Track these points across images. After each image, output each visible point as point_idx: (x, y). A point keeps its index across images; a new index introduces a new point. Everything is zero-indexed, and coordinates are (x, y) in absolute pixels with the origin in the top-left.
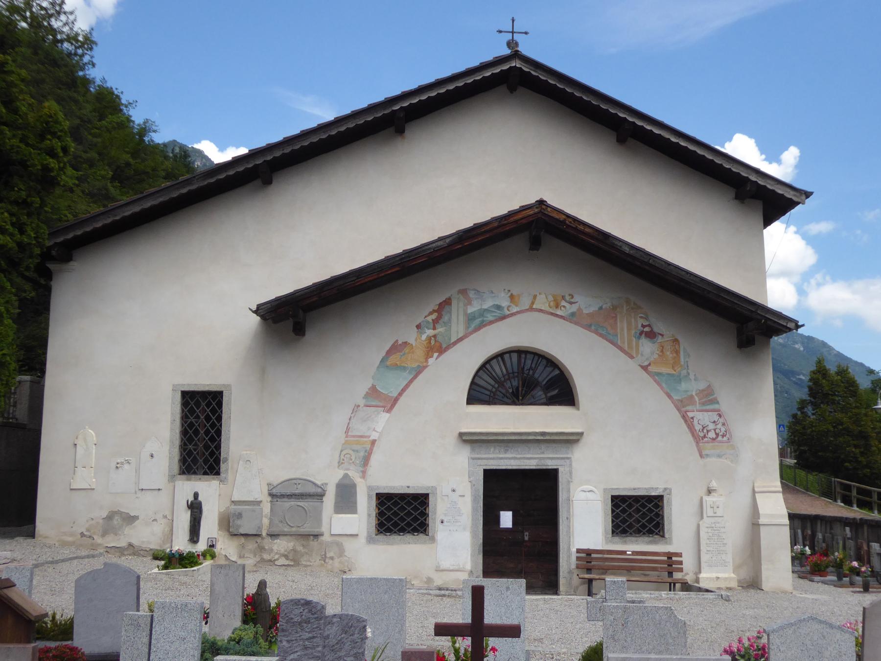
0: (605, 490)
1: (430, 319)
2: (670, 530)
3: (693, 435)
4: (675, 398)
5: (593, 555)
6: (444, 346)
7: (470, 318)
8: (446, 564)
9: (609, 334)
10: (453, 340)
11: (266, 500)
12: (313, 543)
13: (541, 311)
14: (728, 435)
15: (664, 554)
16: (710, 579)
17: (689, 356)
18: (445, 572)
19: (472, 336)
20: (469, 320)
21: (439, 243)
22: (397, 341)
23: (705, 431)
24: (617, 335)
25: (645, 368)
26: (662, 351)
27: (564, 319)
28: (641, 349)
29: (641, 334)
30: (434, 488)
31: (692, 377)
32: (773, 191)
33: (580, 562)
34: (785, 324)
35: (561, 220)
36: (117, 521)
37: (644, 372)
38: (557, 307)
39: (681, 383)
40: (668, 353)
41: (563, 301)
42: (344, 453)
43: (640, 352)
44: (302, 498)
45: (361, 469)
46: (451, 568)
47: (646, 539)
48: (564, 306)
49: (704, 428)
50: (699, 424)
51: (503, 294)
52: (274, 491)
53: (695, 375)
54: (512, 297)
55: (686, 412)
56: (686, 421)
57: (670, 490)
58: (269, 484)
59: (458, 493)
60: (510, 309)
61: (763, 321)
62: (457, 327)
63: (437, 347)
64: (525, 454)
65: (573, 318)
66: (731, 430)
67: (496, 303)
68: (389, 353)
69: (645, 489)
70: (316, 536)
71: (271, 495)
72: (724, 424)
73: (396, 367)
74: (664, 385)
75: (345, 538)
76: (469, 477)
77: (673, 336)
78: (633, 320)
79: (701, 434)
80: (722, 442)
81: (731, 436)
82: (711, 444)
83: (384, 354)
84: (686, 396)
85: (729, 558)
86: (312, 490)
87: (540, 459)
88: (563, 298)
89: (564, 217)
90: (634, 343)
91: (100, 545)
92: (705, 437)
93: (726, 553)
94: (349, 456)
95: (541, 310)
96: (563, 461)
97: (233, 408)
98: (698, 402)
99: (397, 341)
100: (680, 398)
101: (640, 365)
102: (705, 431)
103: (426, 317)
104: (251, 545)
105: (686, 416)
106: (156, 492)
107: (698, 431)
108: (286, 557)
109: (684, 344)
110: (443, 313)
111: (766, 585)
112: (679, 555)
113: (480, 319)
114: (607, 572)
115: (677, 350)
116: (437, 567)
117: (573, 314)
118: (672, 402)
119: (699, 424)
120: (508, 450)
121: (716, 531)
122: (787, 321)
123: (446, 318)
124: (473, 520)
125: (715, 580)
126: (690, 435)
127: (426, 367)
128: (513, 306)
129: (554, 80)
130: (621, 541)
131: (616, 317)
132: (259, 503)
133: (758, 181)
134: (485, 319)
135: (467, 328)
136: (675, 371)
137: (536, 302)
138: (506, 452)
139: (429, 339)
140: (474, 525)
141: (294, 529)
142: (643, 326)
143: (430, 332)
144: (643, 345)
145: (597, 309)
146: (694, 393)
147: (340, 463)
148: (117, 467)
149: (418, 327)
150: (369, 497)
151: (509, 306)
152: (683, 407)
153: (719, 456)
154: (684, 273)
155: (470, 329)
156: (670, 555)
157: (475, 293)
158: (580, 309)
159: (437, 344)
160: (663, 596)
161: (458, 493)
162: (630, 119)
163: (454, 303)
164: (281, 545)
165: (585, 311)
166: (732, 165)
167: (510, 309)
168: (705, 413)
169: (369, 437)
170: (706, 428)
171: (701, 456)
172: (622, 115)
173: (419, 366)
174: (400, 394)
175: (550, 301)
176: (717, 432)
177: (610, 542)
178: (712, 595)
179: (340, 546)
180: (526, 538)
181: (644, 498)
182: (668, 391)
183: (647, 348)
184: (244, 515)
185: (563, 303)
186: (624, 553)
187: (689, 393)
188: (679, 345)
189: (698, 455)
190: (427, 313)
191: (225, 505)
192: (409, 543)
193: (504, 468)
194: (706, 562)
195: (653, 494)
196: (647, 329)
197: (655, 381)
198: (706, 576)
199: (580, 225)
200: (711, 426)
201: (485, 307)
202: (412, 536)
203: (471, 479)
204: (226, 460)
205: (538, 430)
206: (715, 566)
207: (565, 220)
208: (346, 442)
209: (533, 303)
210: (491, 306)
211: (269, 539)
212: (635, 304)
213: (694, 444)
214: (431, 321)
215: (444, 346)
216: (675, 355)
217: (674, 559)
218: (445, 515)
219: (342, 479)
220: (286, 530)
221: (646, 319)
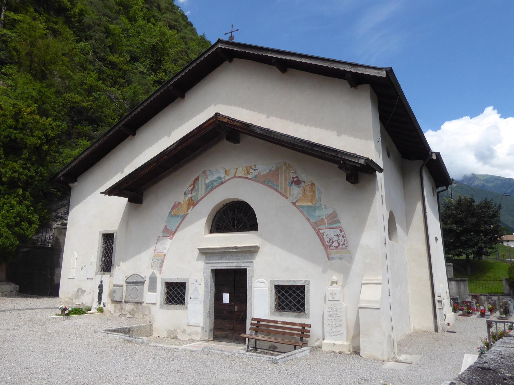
0: (271, 281)
1: (190, 189)
2: (309, 309)
4: (312, 221)
5: (261, 323)
6: (195, 202)
7: (207, 186)
8: (192, 322)
9: (275, 185)
10: (199, 198)
12: (140, 307)
13: (240, 177)
14: (346, 244)
15: (300, 325)
16: (329, 345)
17: (321, 193)
18: (191, 327)
19: (208, 195)
20: (206, 187)
21: (172, 147)
22: (176, 202)
23: (331, 242)
24: (279, 185)
25: (294, 204)
26: (304, 192)
27: (251, 180)
28: (292, 192)
29: (292, 183)
30: (188, 279)
31: (323, 206)
32: (362, 74)
33: (253, 326)
34: (357, 161)
35: (226, 122)
36: (80, 292)
37: (294, 206)
38: (248, 173)
39: (316, 211)
40: (308, 193)
41: (251, 169)
42: (153, 261)
43: (291, 194)
44: (137, 284)
45: (160, 269)
46: (194, 325)
47: (295, 314)
48: (251, 173)
49: (330, 240)
50: (327, 237)
53: (325, 205)
54: (226, 171)
55: (319, 230)
56: (319, 236)
57: (309, 281)
58: (126, 277)
59: (198, 282)
60: (225, 178)
61: (342, 161)
63: (192, 203)
64: (230, 260)
65: (256, 179)
66: (348, 240)
67: (218, 176)
68: (173, 208)
69: (294, 280)
70: (141, 303)
71: (127, 282)
72: (343, 237)
73: (176, 216)
74: (305, 213)
75: (151, 305)
76: (204, 274)
77: (311, 181)
78: (288, 175)
79: (329, 244)
80: (343, 249)
81: (348, 244)
83: (170, 209)
84: (319, 219)
85: (344, 330)
86: (140, 280)
87: (238, 262)
88: (251, 167)
90: (288, 188)
91: (74, 303)
92: (331, 246)
93: (342, 327)
94: (155, 262)
95: (239, 176)
96: (249, 264)
97: (117, 241)
98: (326, 223)
99: (176, 202)
100: (315, 221)
101: (291, 202)
102: (331, 242)
103: (188, 188)
104: (118, 306)
105: (319, 233)
106: (91, 280)
107: (326, 242)
108: (130, 312)
109: (317, 185)
110: (196, 185)
111: (363, 353)
112: (309, 326)
113: (211, 186)
114: (270, 334)
115: (313, 190)
116: (188, 323)
117: (256, 176)
118: (310, 224)
119: (327, 237)
120: (222, 258)
121: (335, 311)
122: (358, 159)
123: (196, 187)
125: (332, 345)
126: (321, 245)
127: (187, 214)
128: (226, 176)
130: (279, 314)
131: (278, 175)
132: (122, 286)
133: (351, 70)
134: (213, 185)
135: (206, 191)
136: (312, 204)
137: (237, 172)
138: (221, 259)
139: (189, 199)
140: (205, 301)
141: (133, 299)
142: (294, 178)
143: (189, 196)
144: (293, 190)
145: (268, 171)
146: (324, 218)
147: (152, 266)
148: (81, 269)
149: (185, 194)
150: (162, 284)
151: (225, 177)
152: (317, 227)
153: (340, 259)
154: (291, 139)
155: (207, 192)
156: (304, 326)
157: (209, 172)
158: (259, 173)
159: (192, 202)
160: (236, 354)
161: (198, 282)
162: (274, 56)
163: (200, 178)
164: (129, 307)
165: (262, 174)
166: (334, 65)
167: (225, 178)
168: (332, 230)
170: (332, 240)
171: (329, 259)
172: (269, 55)
173: (184, 214)
174: (176, 230)
175: (244, 170)
176: (339, 242)
177: (273, 314)
178: (266, 358)
179: (149, 308)
180: (236, 310)
181: (295, 287)
182: (308, 217)
183: (296, 191)
185: (251, 171)
186: (276, 322)
187: (321, 218)
188: (315, 186)
189: (327, 258)
191: (111, 287)
192: (177, 309)
193: (220, 268)
194: (328, 332)
195: (298, 284)
196: (295, 179)
197: (300, 211)
198: (327, 342)
199: (235, 122)
200: (335, 238)
201: (214, 179)
202: (180, 306)
203: (205, 274)
204: (113, 265)
205: (233, 246)
206: (334, 335)
207: (228, 121)
209: (236, 173)
210: (216, 178)
211: (124, 304)
212: (289, 165)
213: (324, 251)
214: (190, 190)
215: (195, 202)
216: (312, 193)
217: (306, 328)
218: (192, 294)
219: (152, 274)
220: (130, 299)
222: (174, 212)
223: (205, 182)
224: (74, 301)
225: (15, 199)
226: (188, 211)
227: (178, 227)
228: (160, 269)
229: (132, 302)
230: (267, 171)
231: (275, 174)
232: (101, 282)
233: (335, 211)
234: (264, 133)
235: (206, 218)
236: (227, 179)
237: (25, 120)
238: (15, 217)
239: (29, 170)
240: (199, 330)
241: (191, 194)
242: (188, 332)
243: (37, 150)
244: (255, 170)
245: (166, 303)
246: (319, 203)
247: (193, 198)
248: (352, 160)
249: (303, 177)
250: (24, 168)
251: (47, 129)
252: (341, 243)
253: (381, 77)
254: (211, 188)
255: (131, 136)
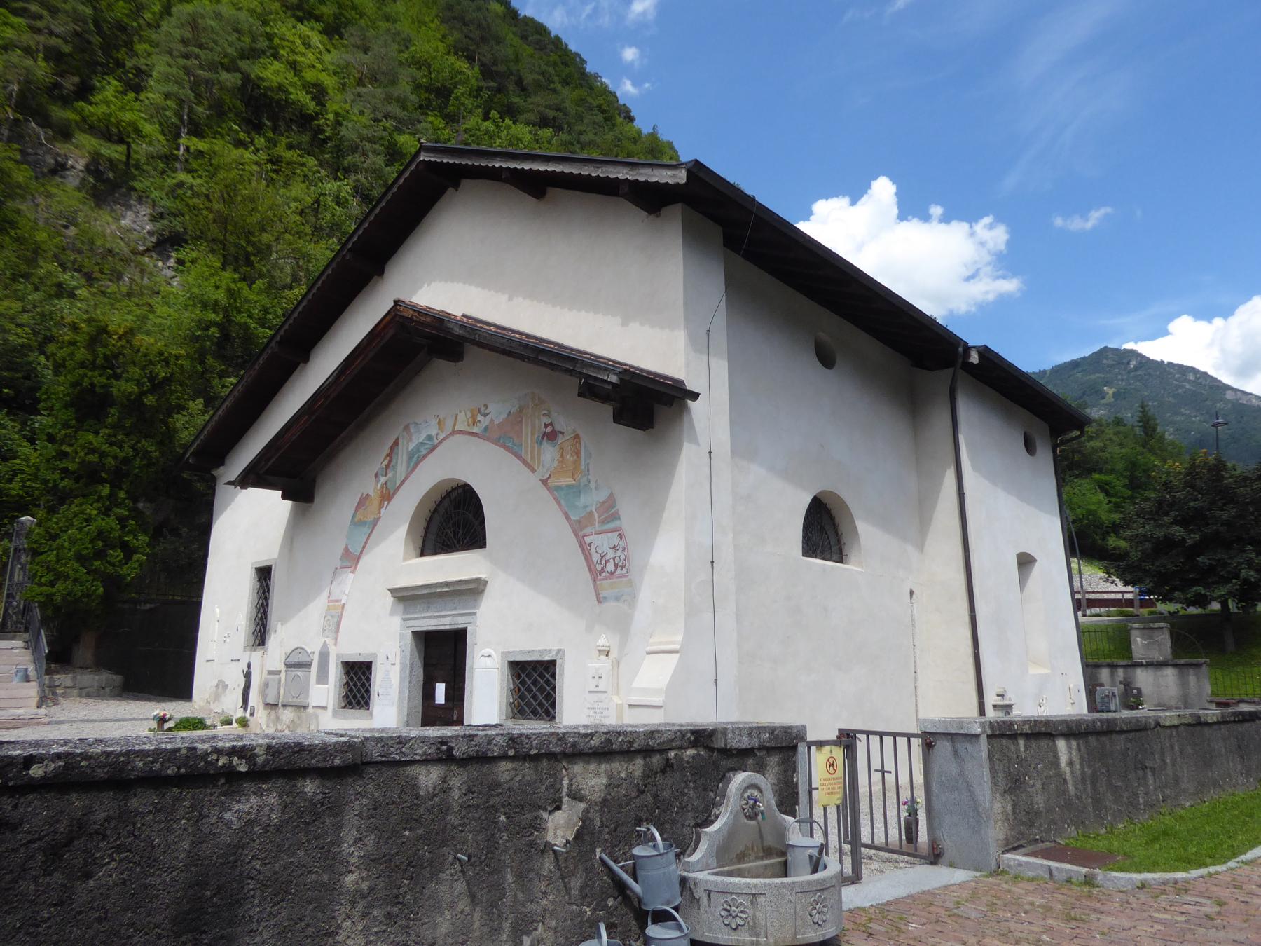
3: (590, 570)
4: (573, 518)
10: (398, 483)
11: (283, 668)
13: (460, 432)
21: (330, 379)
23: (603, 562)
25: (544, 482)
29: (543, 438)
31: (592, 485)
34: (605, 378)
39: (579, 496)
48: (480, 421)
49: (602, 557)
52: (290, 660)
56: (583, 550)
57: (564, 652)
59: (391, 660)
62: (401, 469)
63: (387, 496)
64: (442, 611)
65: (485, 435)
68: (358, 508)
70: (305, 707)
71: (288, 666)
73: (362, 523)
79: (599, 567)
82: (609, 581)
86: (304, 659)
88: (479, 409)
92: (602, 571)
104: (273, 714)
106: (237, 663)
109: (585, 439)
117: (486, 429)
123: (394, 461)
124: (399, 693)
127: (379, 519)
129: (447, 158)
131: (521, 422)
133: (628, 177)
137: (457, 423)
138: (428, 610)
143: (383, 479)
147: (324, 630)
149: (376, 476)
151: (437, 434)
153: (617, 599)
154: (505, 340)
161: (391, 660)
171: (599, 601)
172: (497, 165)
174: (362, 552)
179: (317, 717)
182: (566, 509)
183: (549, 453)
185: (480, 417)
187: (588, 510)
196: (549, 429)
200: (611, 554)
201: (420, 441)
209: (455, 425)
211: (281, 709)
212: (539, 399)
213: (591, 582)
216: (575, 457)
221: (548, 415)
223: (407, 449)
224: (212, 706)
225: (95, 505)
226: (380, 513)
227: (364, 547)
229: (292, 706)
230: (504, 416)
231: (516, 419)
232: (249, 666)
233: (612, 493)
234: (465, 334)
235: (408, 524)
237: (110, 350)
238: (92, 541)
239: (121, 447)
241: (386, 475)
243: (134, 405)
244: (485, 415)
245: (343, 705)
246: (585, 478)
247: (388, 484)
248: (598, 376)
249: (561, 423)
250: (111, 444)
251: (151, 362)
252: (620, 564)
253: (678, 184)
254: (416, 460)
255: (302, 365)
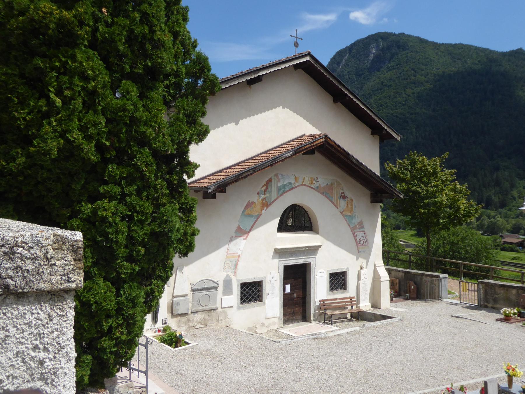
4: (351, 226)
6: (269, 203)
7: (279, 189)
8: (269, 316)
10: (272, 200)
12: (213, 313)
13: (306, 185)
25: (341, 213)
26: (347, 205)
38: (312, 184)
42: (226, 263)
45: (234, 271)
46: (272, 317)
51: (292, 177)
54: (296, 178)
56: (354, 237)
59: (274, 279)
62: (274, 195)
63: (266, 204)
65: (317, 189)
71: (193, 290)
73: (249, 216)
75: (228, 309)
79: (359, 242)
83: (243, 208)
89: (334, 144)
92: (360, 243)
94: (228, 264)
104: (183, 319)
108: (201, 323)
109: (354, 201)
117: (317, 187)
123: (269, 189)
127: (261, 214)
131: (332, 189)
132: (186, 295)
135: (278, 194)
137: (305, 181)
139: (263, 200)
141: (204, 308)
142: (342, 193)
143: (263, 196)
147: (224, 269)
149: (258, 193)
150: (238, 285)
159: (266, 203)
163: (273, 180)
164: (198, 317)
169: (237, 253)
171: (358, 252)
179: (225, 313)
180: (295, 297)
183: (343, 203)
184: (180, 303)
185: (314, 182)
186: (336, 299)
190: (261, 186)
196: (343, 195)
200: (362, 238)
201: (285, 183)
208: (227, 257)
211: (192, 315)
217: (352, 300)
220: (200, 308)
221: (342, 189)
222: (248, 211)
223: (277, 185)
226: (261, 212)
227: (252, 227)
228: (234, 271)
229: (203, 311)
230: (325, 185)
231: (330, 187)
234: (357, 164)
235: (279, 218)
236: (296, 185)
240: (276, 320)
241: (265, 195)
242: (266, 324)
244: (317, 182)
247: (267, 199)
254: (283, 191)
